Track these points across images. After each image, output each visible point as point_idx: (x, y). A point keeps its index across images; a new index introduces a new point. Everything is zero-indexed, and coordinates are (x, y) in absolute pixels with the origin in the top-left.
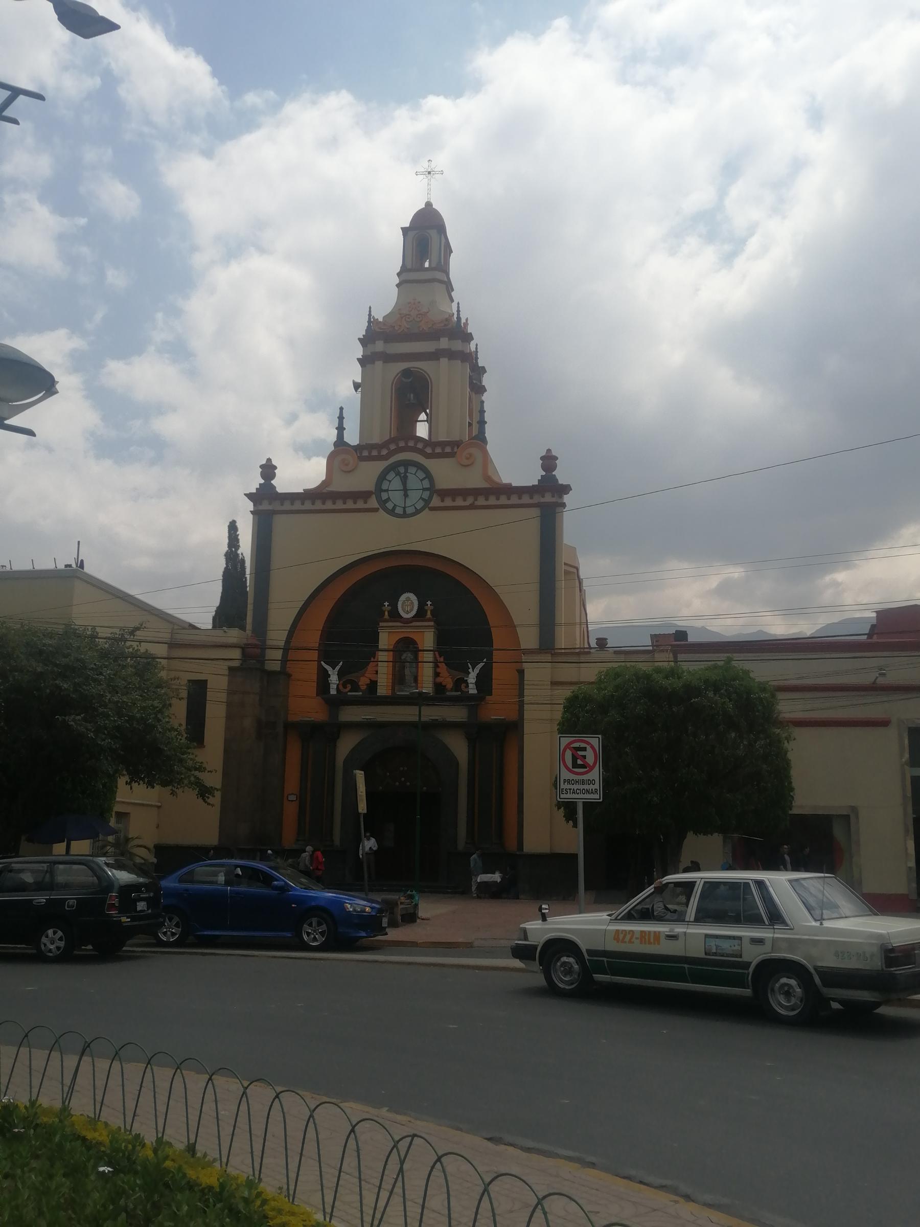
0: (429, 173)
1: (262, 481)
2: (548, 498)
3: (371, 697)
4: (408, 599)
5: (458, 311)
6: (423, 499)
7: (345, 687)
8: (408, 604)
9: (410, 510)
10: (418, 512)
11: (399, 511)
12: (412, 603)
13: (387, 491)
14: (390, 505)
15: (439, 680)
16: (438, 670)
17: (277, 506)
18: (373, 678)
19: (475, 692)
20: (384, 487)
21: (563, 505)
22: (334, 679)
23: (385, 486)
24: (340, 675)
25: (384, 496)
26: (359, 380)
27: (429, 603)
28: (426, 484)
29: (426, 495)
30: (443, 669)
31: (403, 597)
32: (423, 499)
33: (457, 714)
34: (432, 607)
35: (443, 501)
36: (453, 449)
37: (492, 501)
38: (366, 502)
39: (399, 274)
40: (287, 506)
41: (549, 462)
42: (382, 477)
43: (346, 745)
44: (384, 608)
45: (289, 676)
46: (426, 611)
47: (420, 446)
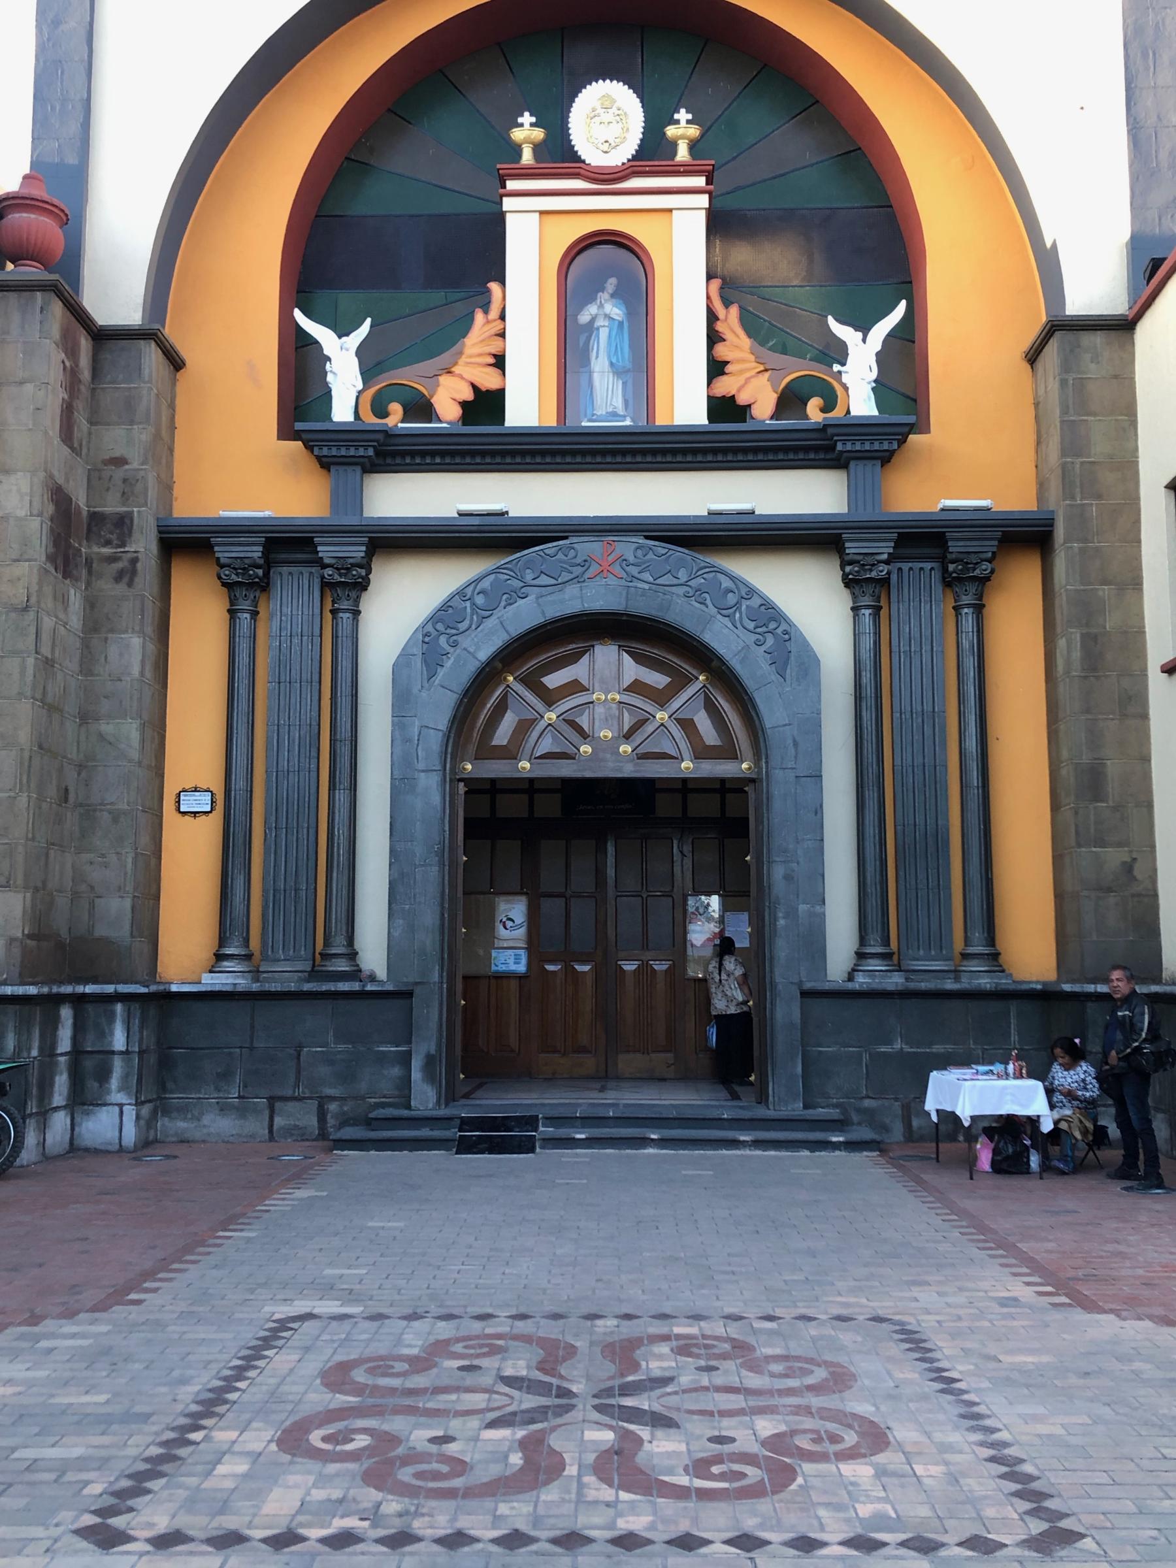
3: (484, 439)
7: (384, 414)
12: (621, 116)
15: (725, 386)
16: (722, 351)
18: (489, 380)
19: (875, 413)
24: (371, 363)
27: (683, 115)
30: (738, 346)
33: (812, 494)
34: (694, 131)
43: (401, 604)
44: (517, 135)
45: (176, 363)
46: (673, 146)
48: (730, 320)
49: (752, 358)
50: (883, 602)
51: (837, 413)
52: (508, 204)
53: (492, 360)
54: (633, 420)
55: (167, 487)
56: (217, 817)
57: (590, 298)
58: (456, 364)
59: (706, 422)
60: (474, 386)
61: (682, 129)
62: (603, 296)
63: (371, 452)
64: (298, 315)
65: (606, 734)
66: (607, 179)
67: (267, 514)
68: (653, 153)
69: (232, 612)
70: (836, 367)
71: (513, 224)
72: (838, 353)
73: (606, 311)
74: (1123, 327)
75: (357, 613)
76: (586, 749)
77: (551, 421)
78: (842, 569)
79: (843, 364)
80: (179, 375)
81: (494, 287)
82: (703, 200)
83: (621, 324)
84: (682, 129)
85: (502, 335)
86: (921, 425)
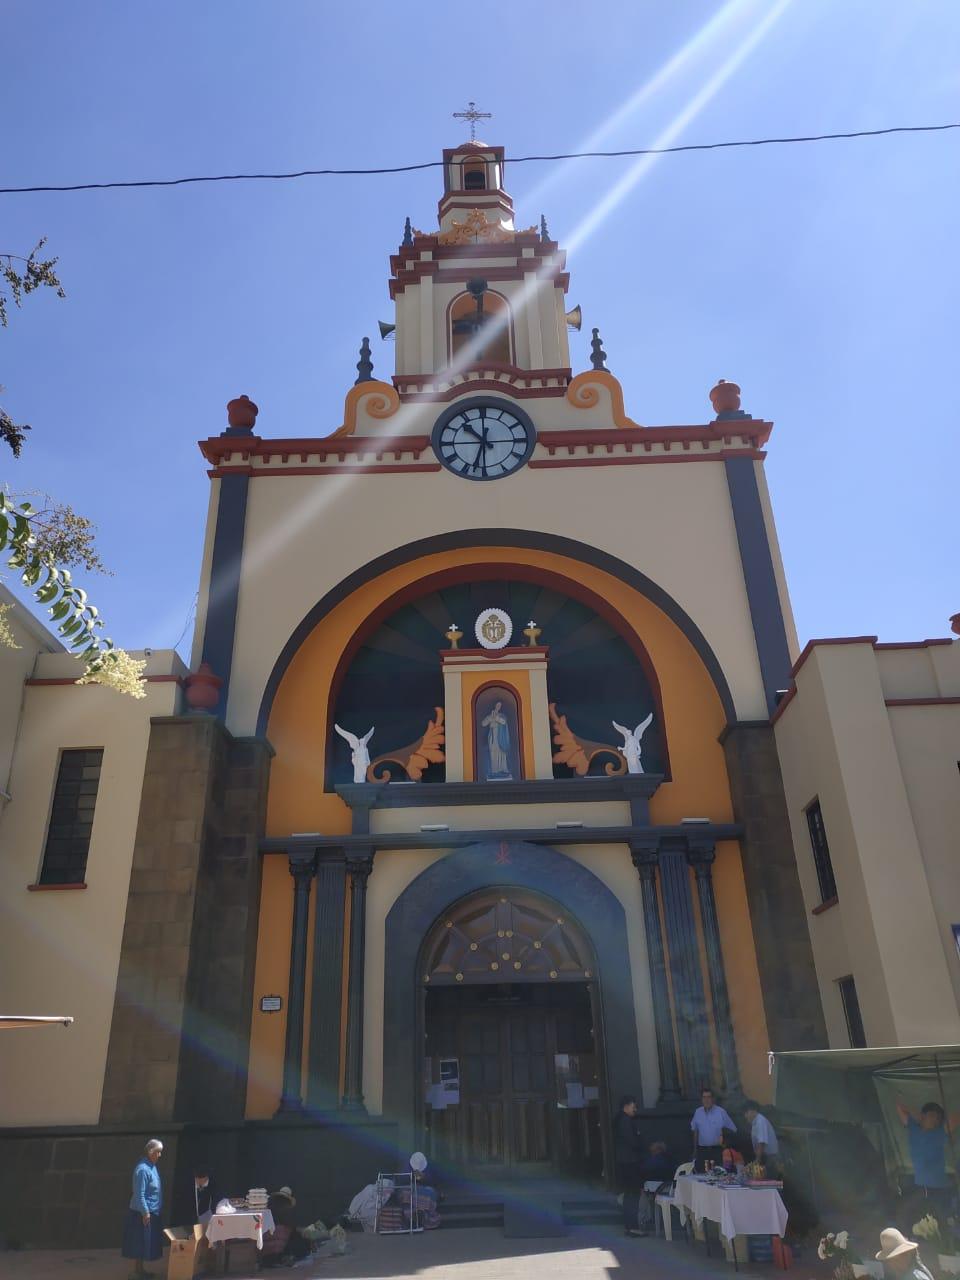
0: (472, 116)
1: (229, 426)
2: (737, 443)
4: (493, 618)
5: (544, 225)
6: (516, 455)
8: (493, 626)
9: (491, 472)
10: (507, 473)
11: (470, 472)
12: (502, 625)
13: (452, 444)
14: (458, 465)
15: (561, 758)
16: (558, 740)
17: (258, 462)
18: (436, 757)
20: (444, 439)
21: (763, 455)
22: (361, 761)
23: (447, 436)
24: (374, 751)
25: (447, 451)
26: (390, 320)
28: (519, 432)
29: (521, 448)
30: (567, 737)
31: (484, 617)
32: (516, 455)
33: (612, 814)
34: (538, 632)
35: (552, 453)
36: (560, 383)
37: (638, 450)
38: (416, 457)
39: (441, 204)
40: (276, 462)
41: (725, 396)
42: (443, 423)
43: (389, 881)
44: (450, 636)
47: (505, 379)
48: (561, 723)
49: (574, 742)
50: (657, 871)
51: (621, 772)
52: (445, 669)
53: (438, 747)
54: (513, 776)
55: (262, 821)
56: (285, 1011)
57: (489, 713)
58: (419, 747)
59: (552, 778)
60: (429, 762)
61: (532, 629)
62: (496, 711)
63: (374, 799)
64: (337, 726)
65: (506, 957)
66: (495, 655)
67: (317, 834)
68: (518, 641)
69: (296, 889)
70: (619, 748)
71: (447, 678)
72: (621, 741)
73: (496, 721)
74: (766, 727)
75: (364, 888)
76: (494, 966)
77: (471, 779)
78: (633, 854)
79: (623, 747)
80: (273, 759)
81: (439, 709)
82: (544, 665)
83: (504, 726)
84: (532, 629)
85: (444, 734)
86: (669, 779)
